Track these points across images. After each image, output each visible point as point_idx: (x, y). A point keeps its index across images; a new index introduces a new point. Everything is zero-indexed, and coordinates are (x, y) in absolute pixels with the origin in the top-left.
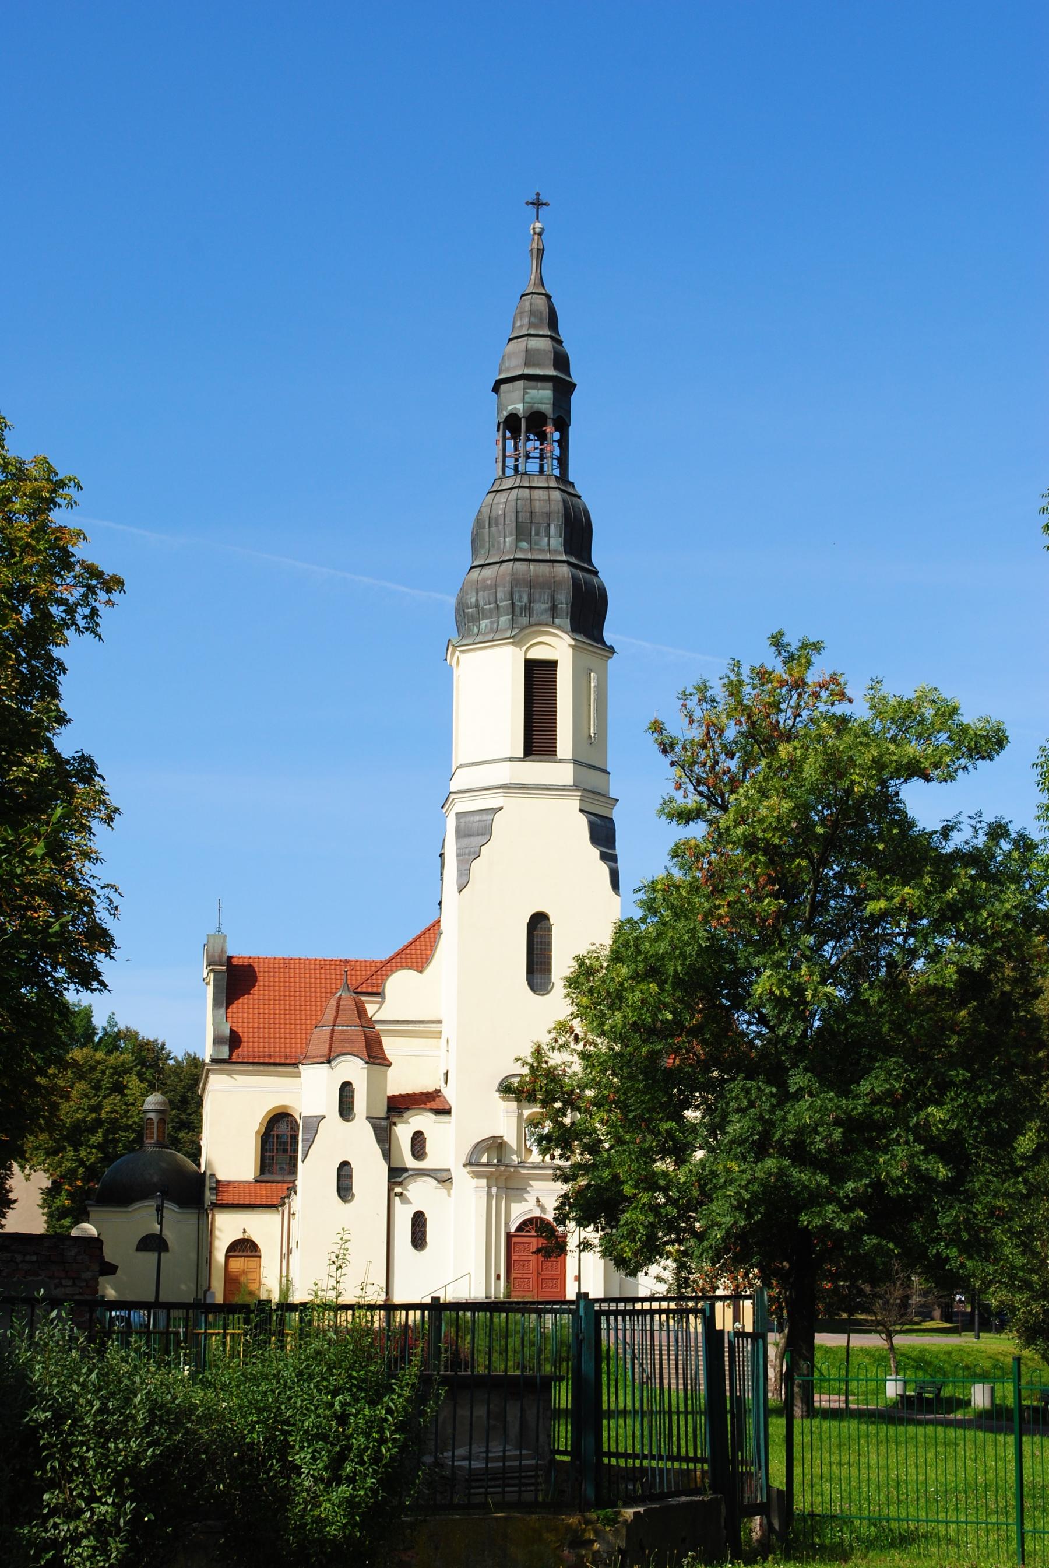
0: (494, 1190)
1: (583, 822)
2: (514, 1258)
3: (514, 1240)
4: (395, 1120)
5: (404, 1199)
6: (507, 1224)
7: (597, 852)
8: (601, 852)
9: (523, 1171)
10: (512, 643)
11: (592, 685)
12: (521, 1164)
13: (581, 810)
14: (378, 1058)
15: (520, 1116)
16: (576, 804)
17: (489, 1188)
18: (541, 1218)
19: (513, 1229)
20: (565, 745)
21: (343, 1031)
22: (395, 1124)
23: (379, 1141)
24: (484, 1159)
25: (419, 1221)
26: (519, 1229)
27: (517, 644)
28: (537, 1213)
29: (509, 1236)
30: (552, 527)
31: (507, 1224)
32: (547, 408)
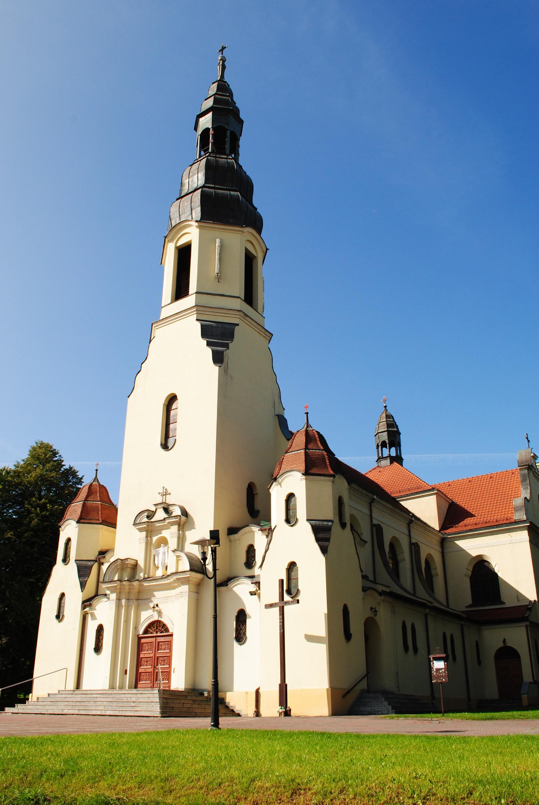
0: (123, 601)
1: (198, 325)
2: (142, 656)
3: (143, 641)
4: (102, 560)
5: (94, 617)
6: (136, 628)
7: (205, 342)
8: (207, 341)
9: (146, 584)
10: (169, 241)
11: (217, 245)
12: (145, 579)
13: (197, 320)
14: (90, 519)
15: (148, 544)
16: (195, 317)
17: (119, 599)
18: (158, 622)
19: (141, 632)
20: (193, 287)
21: (74, 506)
22: (103, 564)
23: (80, 576)
24: (116, 578)
25: (100, 630)
26: (146, 631)
27: (171, 241)
28: (156, 618)
29: (139, 638)
30: (199, 174)
31: (136, 628)
32: (210, 126)
